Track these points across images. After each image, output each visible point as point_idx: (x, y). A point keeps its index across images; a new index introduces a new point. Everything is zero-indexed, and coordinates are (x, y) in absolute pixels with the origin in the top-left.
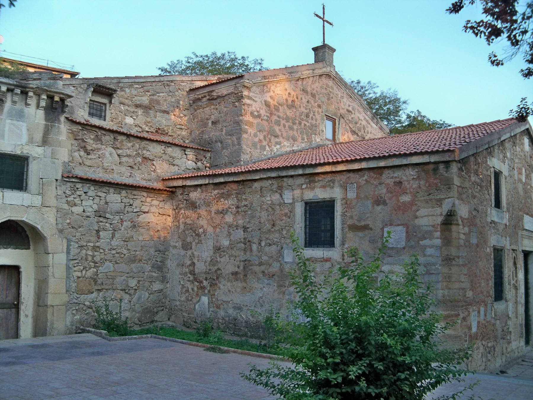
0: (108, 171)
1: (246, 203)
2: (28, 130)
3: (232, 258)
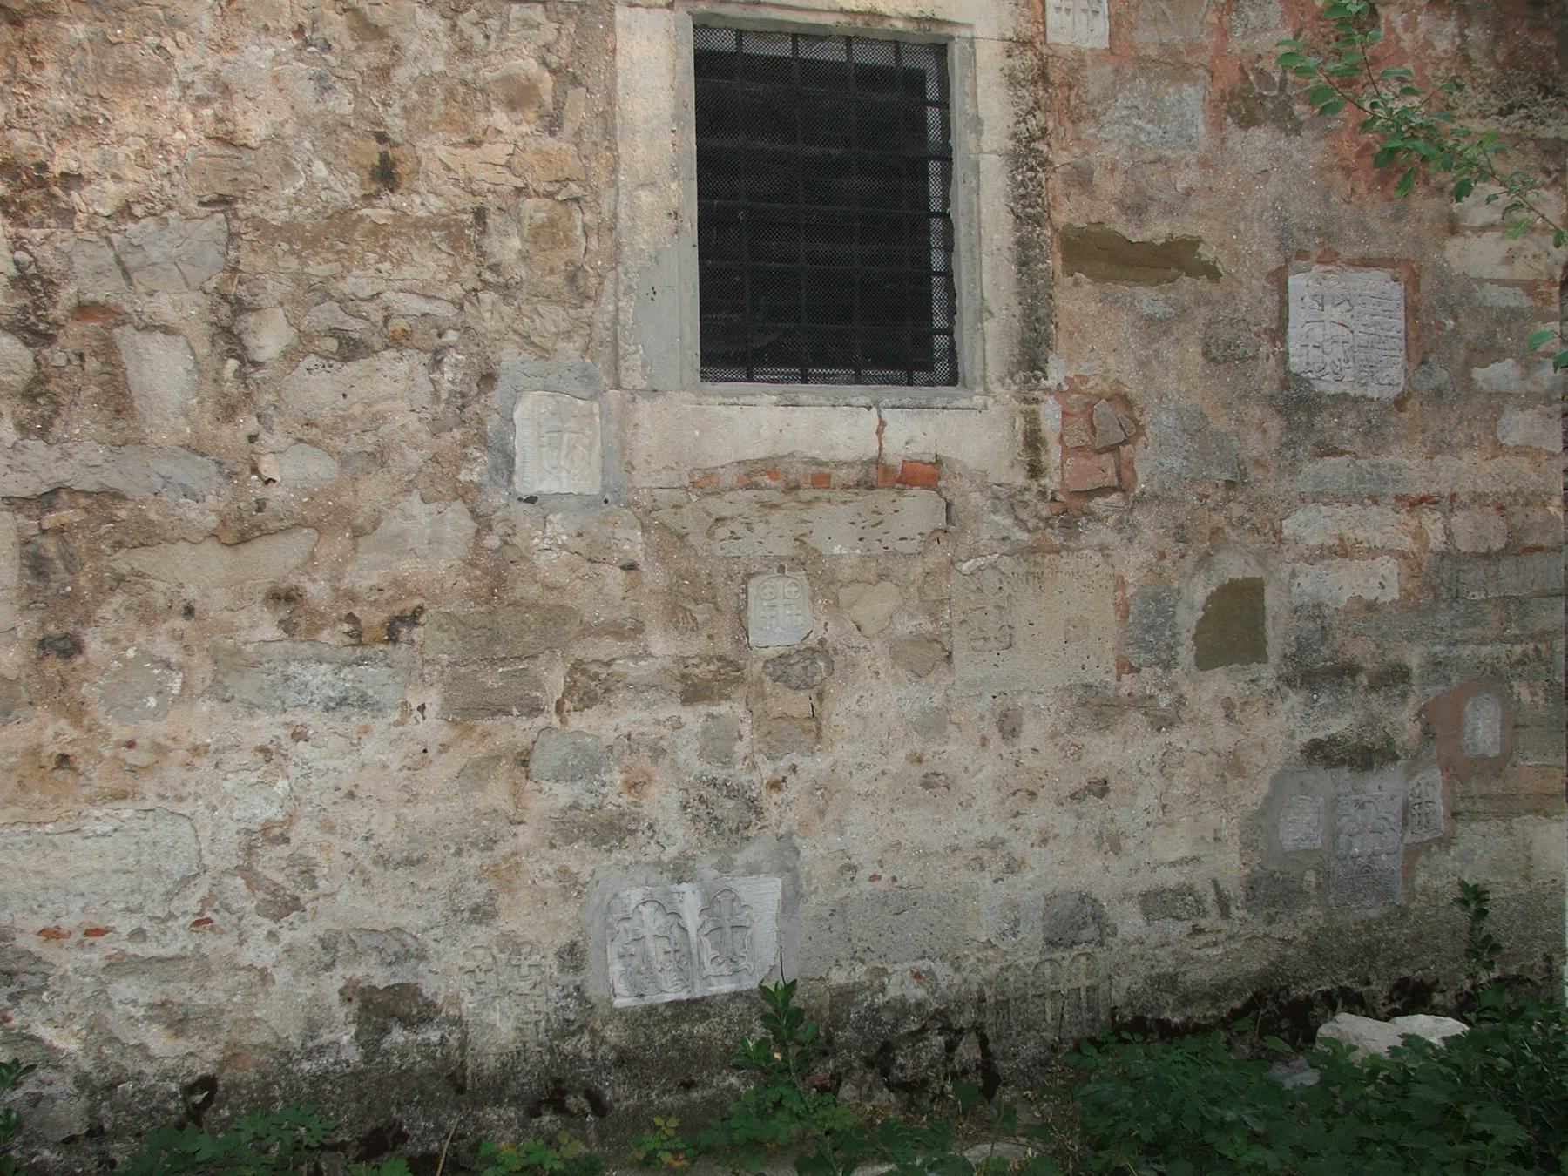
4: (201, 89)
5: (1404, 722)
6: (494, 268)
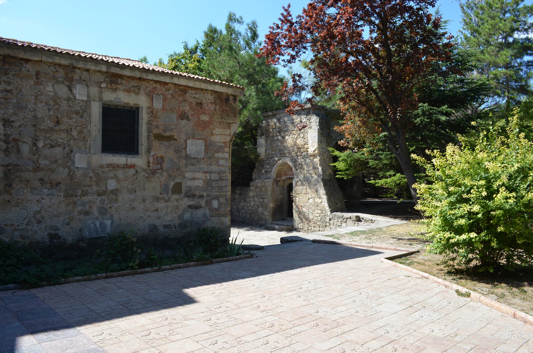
1: (9, 88)
4: (32, 110)
5: (203, 203)
6: (73, 136)
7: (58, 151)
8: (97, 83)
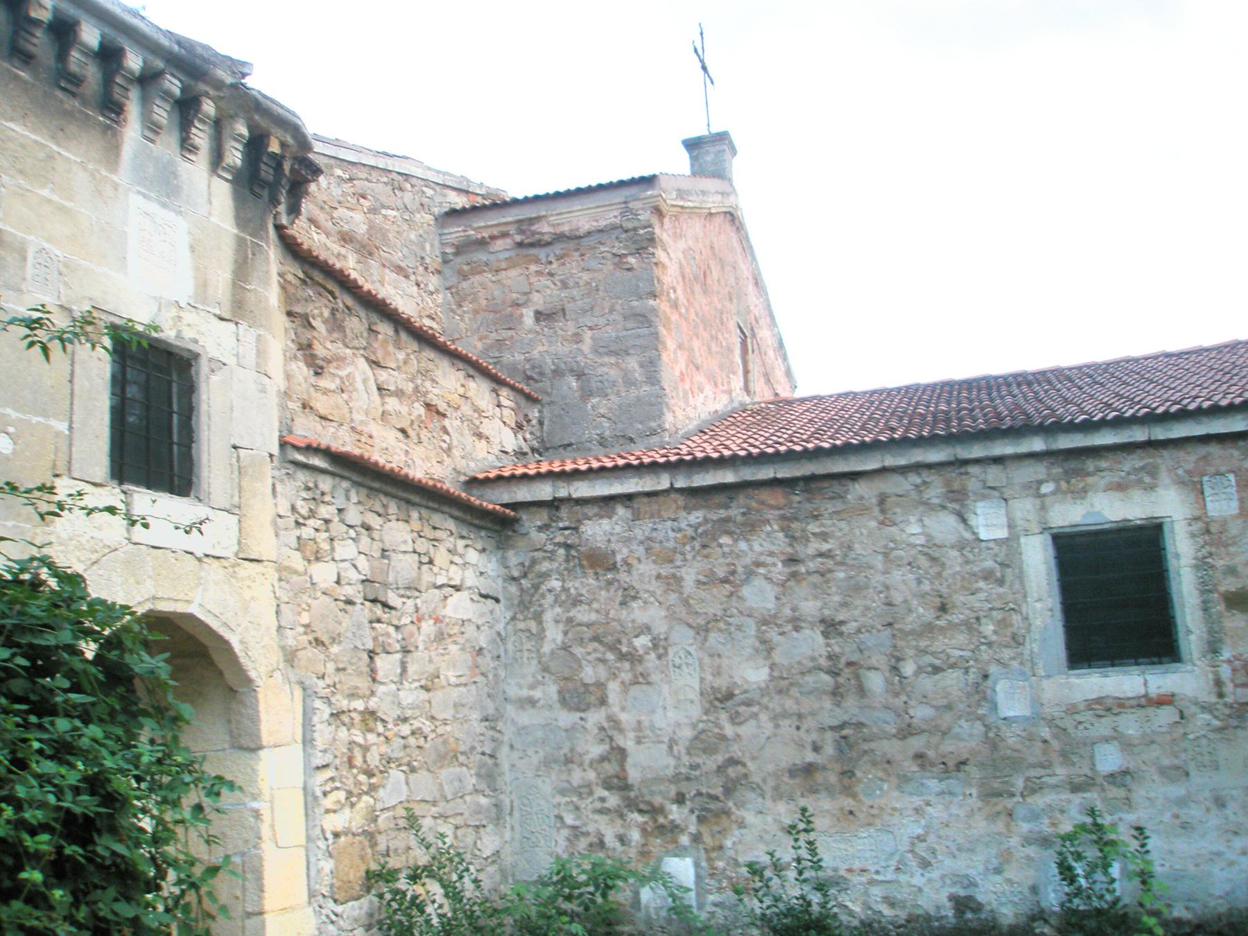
0: (363, 439)
1: (825, 547)
2: (192, 249)
3: (785, 723)
4: (880, 588)
6: (985, 637)
7: (952, 680)
8: (1027, 486)
